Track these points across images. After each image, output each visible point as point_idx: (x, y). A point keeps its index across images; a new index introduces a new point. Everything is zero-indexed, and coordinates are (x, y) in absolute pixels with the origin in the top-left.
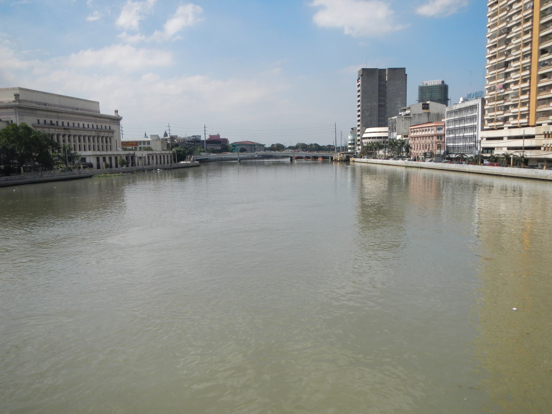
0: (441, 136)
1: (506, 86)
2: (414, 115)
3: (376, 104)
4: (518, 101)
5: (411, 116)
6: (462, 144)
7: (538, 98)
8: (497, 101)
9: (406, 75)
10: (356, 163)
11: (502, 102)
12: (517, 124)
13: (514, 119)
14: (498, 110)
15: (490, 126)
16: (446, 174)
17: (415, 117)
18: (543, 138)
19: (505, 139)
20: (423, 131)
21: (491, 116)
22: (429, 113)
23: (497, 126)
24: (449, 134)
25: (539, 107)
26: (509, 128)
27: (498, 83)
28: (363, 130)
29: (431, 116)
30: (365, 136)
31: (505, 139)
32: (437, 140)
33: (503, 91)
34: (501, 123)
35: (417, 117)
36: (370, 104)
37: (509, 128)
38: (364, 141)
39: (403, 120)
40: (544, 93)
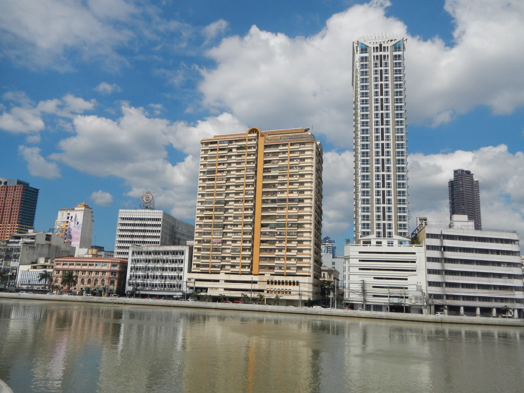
0: (115, 272)
1: (224, 242)
2: (38, 245)
4: (240, 255)
5: (35, 245)
6: (159, 283)
7: (260, 256)
8: (212, 251)
11: (220, 253)
12: (239, 271)
13: (231, 267)
14: (217, 259)
15: (201, 270)
16: (168, 310)
17: (38, 247)
18: (267, 284)
19: (222, 282)
21: (202, 262)
22: (50, 245)
23: (211, 271)
24: (136, 272)
25: (261, 262)
26: (226, 273)
27: (213, 238)
31: (222, 282)
33: (221, 245)
34: (219, 269)
35: (40, 246)
37: (226, 273)
39: (27, 250)
40: (266, 253)
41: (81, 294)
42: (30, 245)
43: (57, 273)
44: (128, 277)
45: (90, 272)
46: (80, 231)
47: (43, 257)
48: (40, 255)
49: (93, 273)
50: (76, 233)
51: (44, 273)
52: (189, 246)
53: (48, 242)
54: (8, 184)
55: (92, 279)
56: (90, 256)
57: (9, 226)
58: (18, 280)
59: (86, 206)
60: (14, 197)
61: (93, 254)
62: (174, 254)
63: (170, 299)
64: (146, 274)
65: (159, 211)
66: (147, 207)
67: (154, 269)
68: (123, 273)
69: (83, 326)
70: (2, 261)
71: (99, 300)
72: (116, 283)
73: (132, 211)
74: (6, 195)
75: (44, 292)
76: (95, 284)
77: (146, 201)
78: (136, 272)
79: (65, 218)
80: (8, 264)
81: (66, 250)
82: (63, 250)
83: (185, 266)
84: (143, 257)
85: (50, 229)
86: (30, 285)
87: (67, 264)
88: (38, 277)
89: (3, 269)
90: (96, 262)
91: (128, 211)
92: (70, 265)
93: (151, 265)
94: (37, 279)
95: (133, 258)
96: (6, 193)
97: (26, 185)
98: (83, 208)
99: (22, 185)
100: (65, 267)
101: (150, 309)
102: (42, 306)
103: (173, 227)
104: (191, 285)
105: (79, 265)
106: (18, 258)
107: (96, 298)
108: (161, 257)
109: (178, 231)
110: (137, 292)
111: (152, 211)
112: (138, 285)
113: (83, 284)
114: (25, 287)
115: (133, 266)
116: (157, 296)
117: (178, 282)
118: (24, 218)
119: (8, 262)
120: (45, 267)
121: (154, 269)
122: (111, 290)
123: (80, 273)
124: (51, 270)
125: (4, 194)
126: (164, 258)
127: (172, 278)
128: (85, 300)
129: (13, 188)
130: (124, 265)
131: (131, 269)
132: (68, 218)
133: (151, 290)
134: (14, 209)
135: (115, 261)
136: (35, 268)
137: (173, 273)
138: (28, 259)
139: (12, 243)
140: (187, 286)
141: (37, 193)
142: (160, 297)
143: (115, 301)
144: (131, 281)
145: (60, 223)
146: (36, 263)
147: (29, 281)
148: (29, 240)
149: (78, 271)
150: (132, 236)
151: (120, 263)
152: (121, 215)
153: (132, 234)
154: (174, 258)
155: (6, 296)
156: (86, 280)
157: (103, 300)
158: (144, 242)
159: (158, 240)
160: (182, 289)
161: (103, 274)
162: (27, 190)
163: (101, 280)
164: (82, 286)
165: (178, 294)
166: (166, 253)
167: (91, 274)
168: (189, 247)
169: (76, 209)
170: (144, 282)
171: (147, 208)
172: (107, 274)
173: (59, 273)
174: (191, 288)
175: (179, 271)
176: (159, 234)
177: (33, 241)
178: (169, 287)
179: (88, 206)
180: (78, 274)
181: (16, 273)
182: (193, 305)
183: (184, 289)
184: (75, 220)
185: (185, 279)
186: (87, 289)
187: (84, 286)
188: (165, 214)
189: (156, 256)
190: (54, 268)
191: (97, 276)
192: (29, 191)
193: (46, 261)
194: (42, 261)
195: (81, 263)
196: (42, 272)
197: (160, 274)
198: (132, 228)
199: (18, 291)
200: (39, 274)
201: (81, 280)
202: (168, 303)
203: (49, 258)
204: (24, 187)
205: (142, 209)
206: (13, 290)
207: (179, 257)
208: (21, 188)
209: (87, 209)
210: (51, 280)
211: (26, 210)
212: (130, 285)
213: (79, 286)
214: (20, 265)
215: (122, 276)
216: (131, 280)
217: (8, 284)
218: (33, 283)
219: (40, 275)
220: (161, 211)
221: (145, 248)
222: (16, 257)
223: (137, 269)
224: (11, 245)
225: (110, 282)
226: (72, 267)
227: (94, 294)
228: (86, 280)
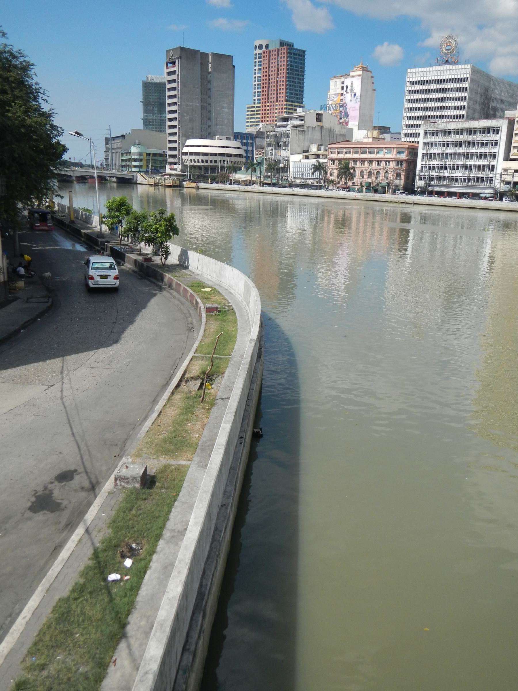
0: (402, 162)
2: (308, 127)
3: (197, 104)
5: (305, 129)
6: (461, 175)
9: (234, 67)
10: (200, 190)
16: (472, 213)
20: (365, 152)
24: (429, 160)
28: (183, 142)
29: (324, 131)
30: (185, 150)
32: (396, 167)
35: (311, 129)
36: (191, 104)
38: (184, 157)
41: (360, 190)
42: (300, 129)
43: (331, 164)
44: (419, 167)
45: (371, 161)
46: (357, 106)
47: (315, 143)
48: (312, 142)
49: (374, 162)
50: (354, 109)
51: (317, 164)
52: (508, 118)
53: (319, 123)
54: (270, 48)
55: (372, 171)
56: (370, 140)
57: (276, 105)
58: (291, 174)
59: (364, 69)
60: (278, 65)
61: (373, 138)
62: (484, 133)
63: (475, 199)
64: (443, 163)
65: (466, 66)
66: (447, 61)
67: (454, 156)
68: (412, 162)
69: (365, 229)
70: (272, 150)
71: (381, 198)
72: (403, 177)
73: (425, 69)
74: (269, 64)
75: (320, 188)
76: (377, 178)
77: (446, 52)
78: (429, 160)
79: (339, 89)
80: (279, 154)
81: (342, 133)
82: (337, 134)
83: (501, 150)
84: (440, 139)
85: (321, 105)
86: (303, 178)
87: (342, 152)
88: (311, 169)
89: (274, 160)
90: (377, 148)
91: (420, 70)
92: (346, 153)
93: (450, 150)
94: (311, 172)
95: (425, 141)
96: (269, 60)
97: (290, 45)
98: (360, 72)
99: (285, 47)
100: (341, 156)
101: (447, 212)
102: (317, 205)
103: (486, 90)
104: (508, 178)
105: (356, 152)
106: (287, 146)
107: (378, 196)
108: (466, 137)
109: (494, 96)
110: (431, 189)
111: (454, 67)
112: (431, 178)
113: (363, 178)
114: (298, 181)
115: (425, 152)
116: (458, 194)
117: (488, 174)
118: (292, 94)
119: (278, 150)
120: (318, 156)
121: (454, 156)
122: (397, 186)
123: (359, 163)
124: (325, 160)
125: (267, 62)
126: (469, 140)
127: (479, 168)
128: (365, 198)
129: (276, 53)
130: (413, 151)
131: (423, 156)
132: (342, 88)
133: (449, 186)
134: (280, 81)
135: (401, 146)
136: (307, 157)
137: (481, 160)
138: (299, 146)
139: (279, 126)
140: (502, 181)
141: (304, 56)
142: (461, 195)
143: (401, 200)
144: (422, 174)
145: (333, 96)
146: (307, 151)
147: (302, 174)
148: (298, 123)
149: (355, 161)
150: (425, 109)
151: (408, 148)
152: (410, 78)
153: (425, 105)
154: (483, 140)
155: (280, 192)
156: (366, 173)
157: (387, 198)
158: (442, 117)
159: (463, 112)
160: (493, 184)
161: (386, 164)
162: (291, 54)
163: (384, 172)
164: (361, 180)
165: (487, 191)
166: (472, 131)
167: (372, 165)
168: (507, 120)
169: (352, 74)
170: (440, 175)
171: (447, 62)
172: (392, 165)
173: (334, 164)
174: (508, 183)
175: (491, 157)
176: (464, 103)
177: (303, 122)
178: (474, 182)
179: (367, 68)
180: (356, 164)
181: (288, 164)
182: (509, 207)
183: (498, 184)
184: (351, 90)
185: (499, 170)
186: (368, 185)
187: (364, 180)
188: (474, 70)
189: (457, 137)
190: (328, 157)
191: (379, 167)
192: (294, 54)
193: (319, 149)
194: (314, 149)
195: (359, 150)
196: (315, 164)
197: (462, 163)
198: (426, 97)
199: (291, 186)
200: (312, 166)
201: (360, 172)
202: (471, 204)
203: (321, 145)
204: (288, 49)
205: (440, 65)
206: (287, 185)
207: (492, 137)
208: (285, 51)
209: (365, 73)
210: (326, 173)
211: (293, 82)
212: (421, 178)
213: (358, 180)
214: (290, 154)
215: (411, 167)
216: (422, 172)
217: (280, 177)
218: (306, 177)
219: (313, 167)
220: (469, 66)
221: (442, 125)
222: (286, 145)
223: (431, 156)
224: (279, 129)
225: (395, 175)
226: (348, 156)
227: (376, 191)
228: (366, 173)
